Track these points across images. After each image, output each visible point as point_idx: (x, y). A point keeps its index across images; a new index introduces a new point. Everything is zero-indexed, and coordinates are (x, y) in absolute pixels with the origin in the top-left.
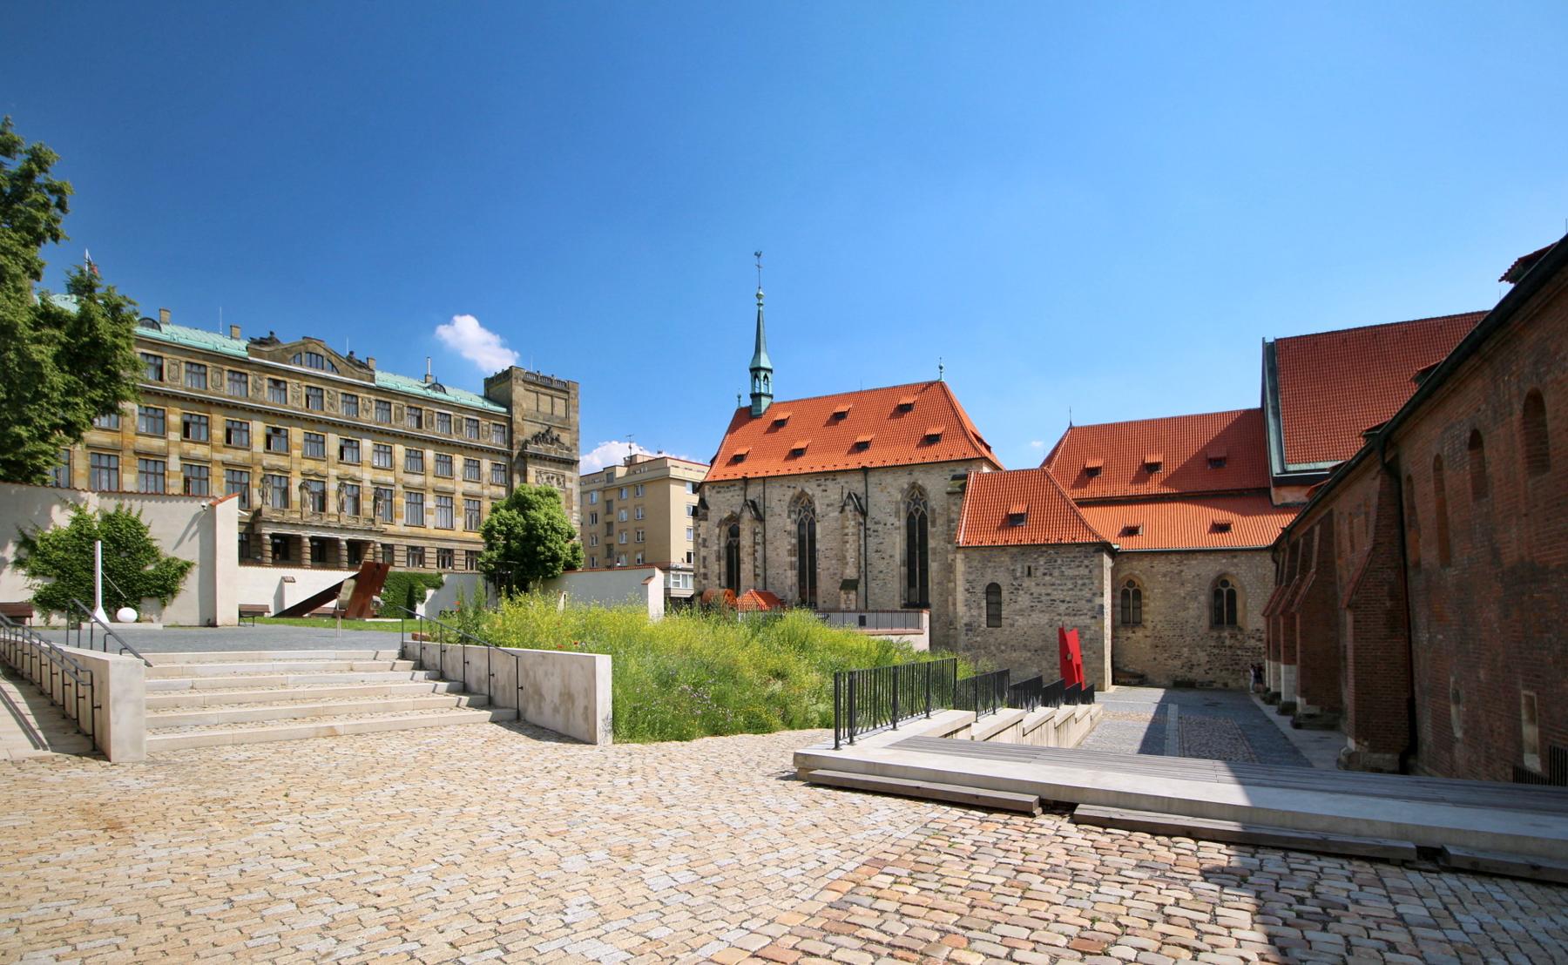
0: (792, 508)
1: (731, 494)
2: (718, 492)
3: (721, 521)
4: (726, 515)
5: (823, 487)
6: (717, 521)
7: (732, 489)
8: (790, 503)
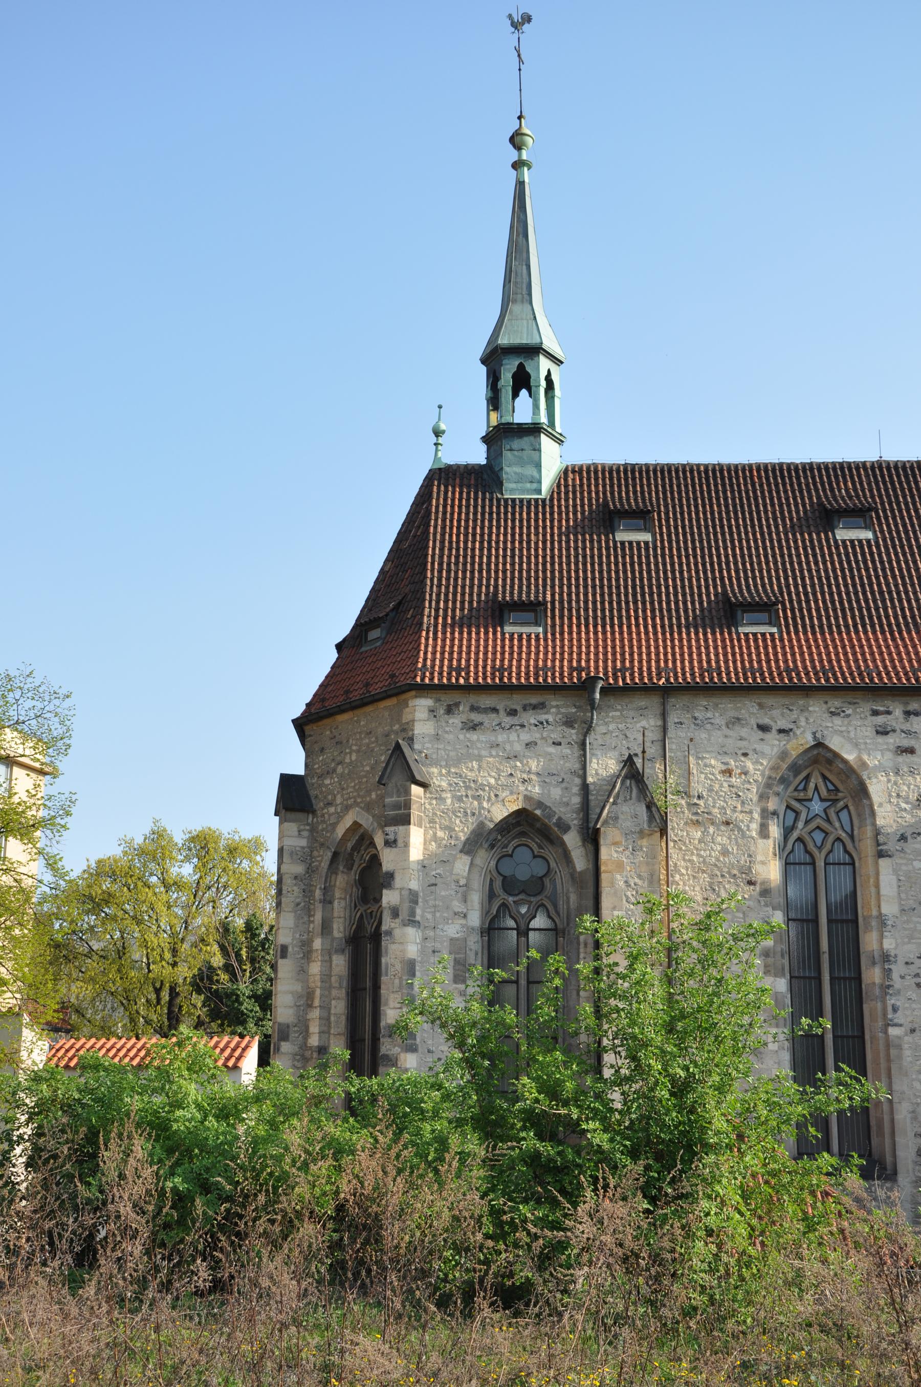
0: (772, 805)
1: (525, 737)
2: (474, 727)
3: (481, 825)
4: (499, 813)
5: (906, 743)
6: (463, 831)
7: (531, 718)
8: (768, 786)
